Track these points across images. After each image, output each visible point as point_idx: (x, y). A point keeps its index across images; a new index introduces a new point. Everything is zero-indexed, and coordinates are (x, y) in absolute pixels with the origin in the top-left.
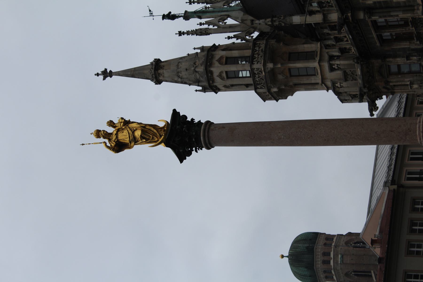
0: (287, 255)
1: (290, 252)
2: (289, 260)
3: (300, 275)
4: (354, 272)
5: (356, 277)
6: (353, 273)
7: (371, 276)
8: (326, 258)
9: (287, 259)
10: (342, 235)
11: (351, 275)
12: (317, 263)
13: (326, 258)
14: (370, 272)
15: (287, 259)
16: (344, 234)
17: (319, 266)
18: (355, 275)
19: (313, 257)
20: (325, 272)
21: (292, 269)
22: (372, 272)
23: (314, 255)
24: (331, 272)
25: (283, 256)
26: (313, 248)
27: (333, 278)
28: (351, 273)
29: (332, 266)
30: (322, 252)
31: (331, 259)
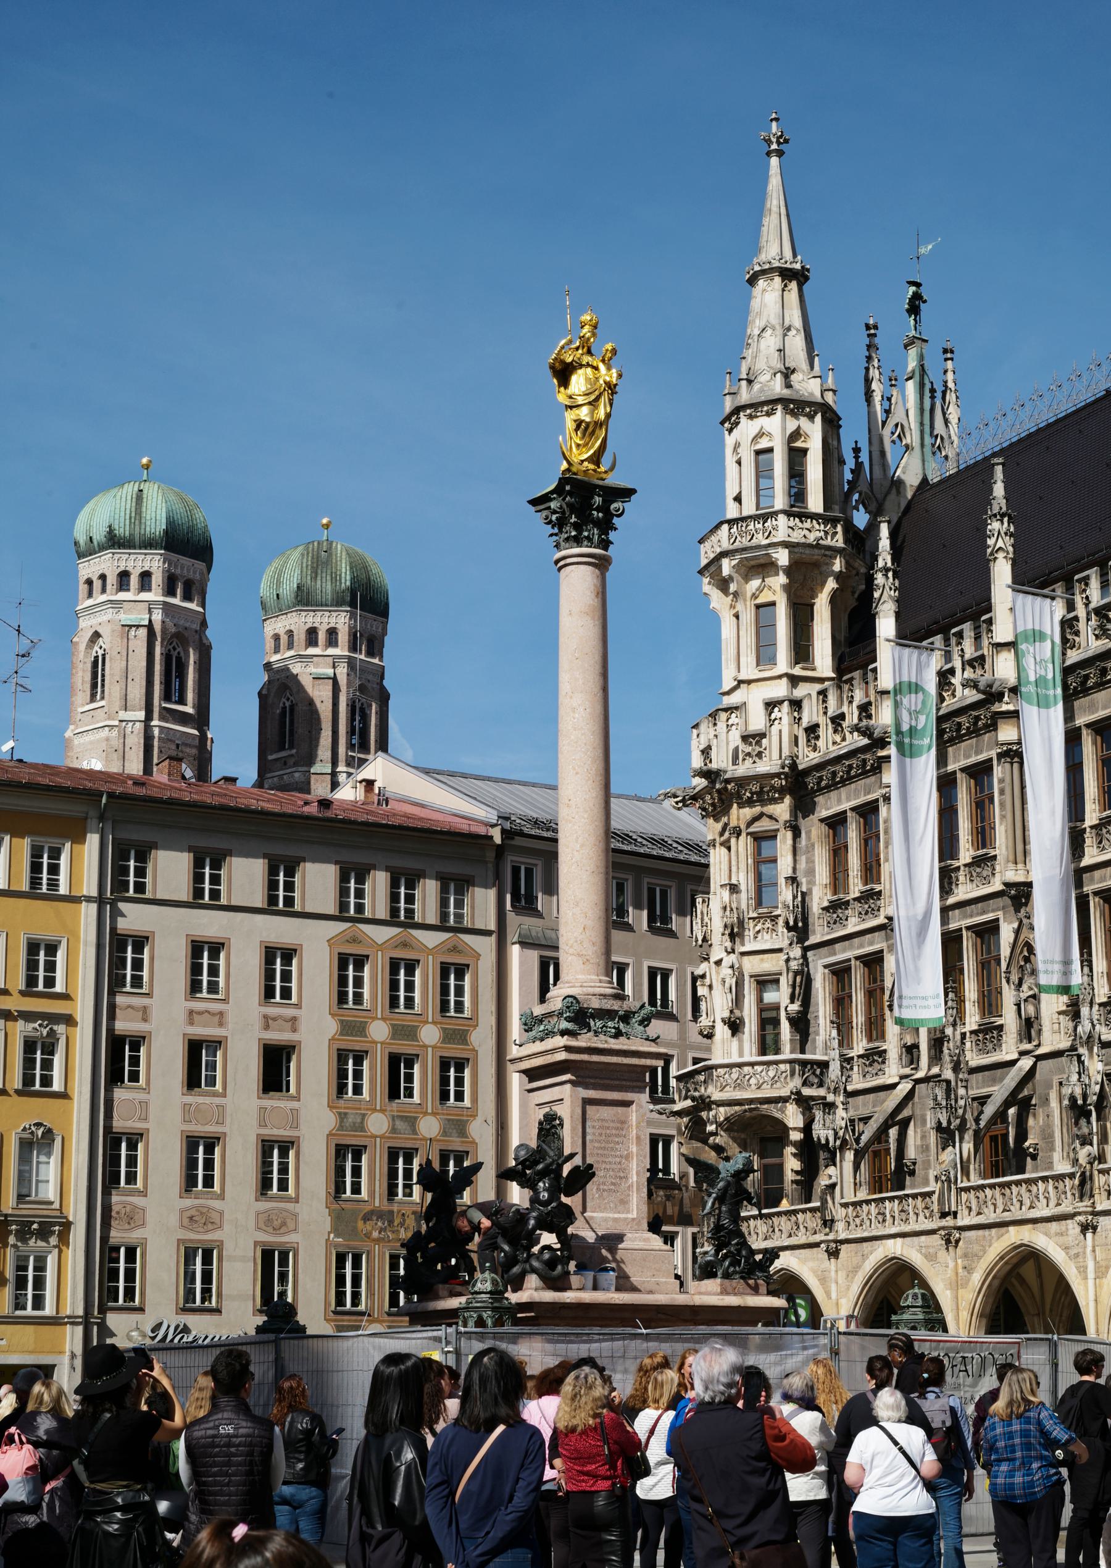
6: (288, 704)
8: (322, 636)
10: (382, 677)
11: (284, 700)
13: (322, 636)
14: (291, 747)
16: (385, 683)
18: (284, 708)
19: (327, 605)
20: (290, 634)
22: (294, 751)
28: (288, 699)
29: (306, 648)
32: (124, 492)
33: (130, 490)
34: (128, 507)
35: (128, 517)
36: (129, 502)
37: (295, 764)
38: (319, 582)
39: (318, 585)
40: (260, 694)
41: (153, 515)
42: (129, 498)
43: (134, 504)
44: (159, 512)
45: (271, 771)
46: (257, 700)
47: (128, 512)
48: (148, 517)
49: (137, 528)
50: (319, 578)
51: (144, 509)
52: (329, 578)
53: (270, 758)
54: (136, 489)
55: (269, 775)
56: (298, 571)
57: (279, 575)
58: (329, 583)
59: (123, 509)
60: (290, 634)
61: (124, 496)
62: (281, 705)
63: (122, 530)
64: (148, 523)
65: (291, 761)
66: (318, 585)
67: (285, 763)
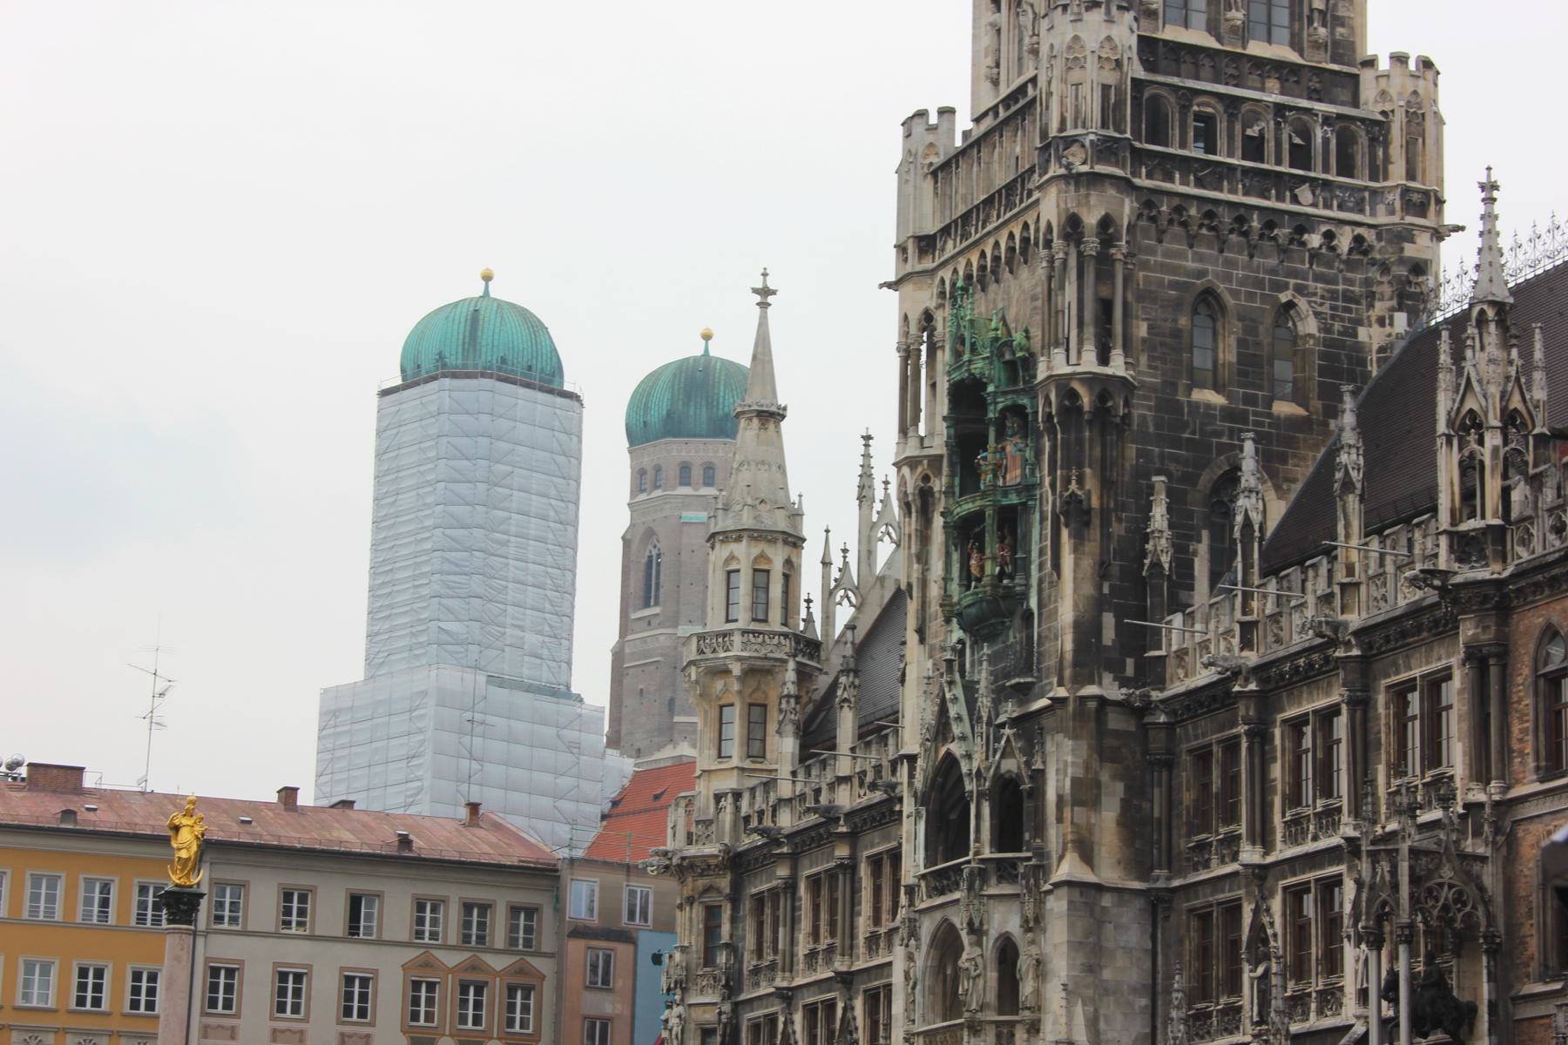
0: (712, 353)
1: (718, 364)
2: (696, 359)
3: (649, 394)
4: (659, 556)
5: (644, 560)
6: (654, 552)
7: (647, 605)
8: (697, 473)
9: (696, 350)
11: (650, 547)
12: (685, 446)
13: (697, 473)
14: (657, 604)
15: (699, 352)
17: (675, 453)
18: (650, 557)
19: (701, 436)
20: (658, 469)
21: (667, 366)
22: (657, 610)
23: (707, 437)
24: (657, 487)
25: (707, 337)
26: (727, 436)
27: (642, 491)
29: (674, 489)
30: (715, 461)
31: (696, 490)
32: (458, 313)
33: (465, 310)
34: (462, 329)
35: (461, 342)
36: (462, 325)
37: (661, 625)
38: (692, 409)
39: (692, 413)
40: (623, 538)
41: (490, 340)
42: (463, 320)
43: (468, 328)
44: (496, 337)
45: (633, 632)
46: (621, 543)
47: (461, 337)
48: (484, 343)
49: (471, 355)
50: (692, 404)
51: (479, 334)
52: (704, 403)
53: (634, 616)
54: (472, 309)
55: (630, 637)
56: (668, 396)
57: (647, 399)
58: (704, 409)
59: (455, 333)
60: (658, 469)
61: (457, 318)
62: (648, 553)
63: (453, 358)
64: (484, 350)
65: (655, 622)
66: (692, 413)
67: (649, 624)
